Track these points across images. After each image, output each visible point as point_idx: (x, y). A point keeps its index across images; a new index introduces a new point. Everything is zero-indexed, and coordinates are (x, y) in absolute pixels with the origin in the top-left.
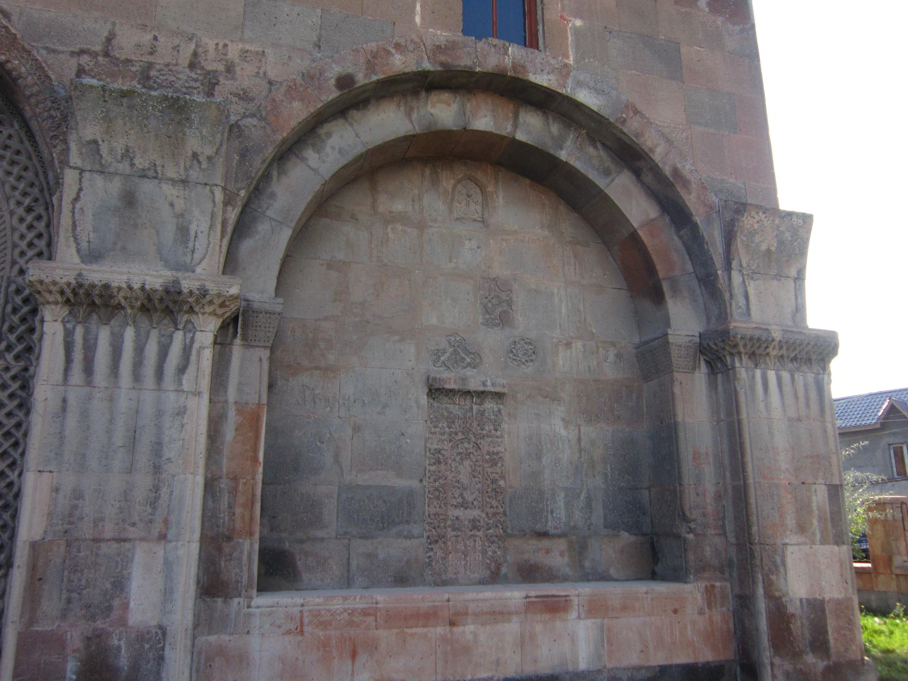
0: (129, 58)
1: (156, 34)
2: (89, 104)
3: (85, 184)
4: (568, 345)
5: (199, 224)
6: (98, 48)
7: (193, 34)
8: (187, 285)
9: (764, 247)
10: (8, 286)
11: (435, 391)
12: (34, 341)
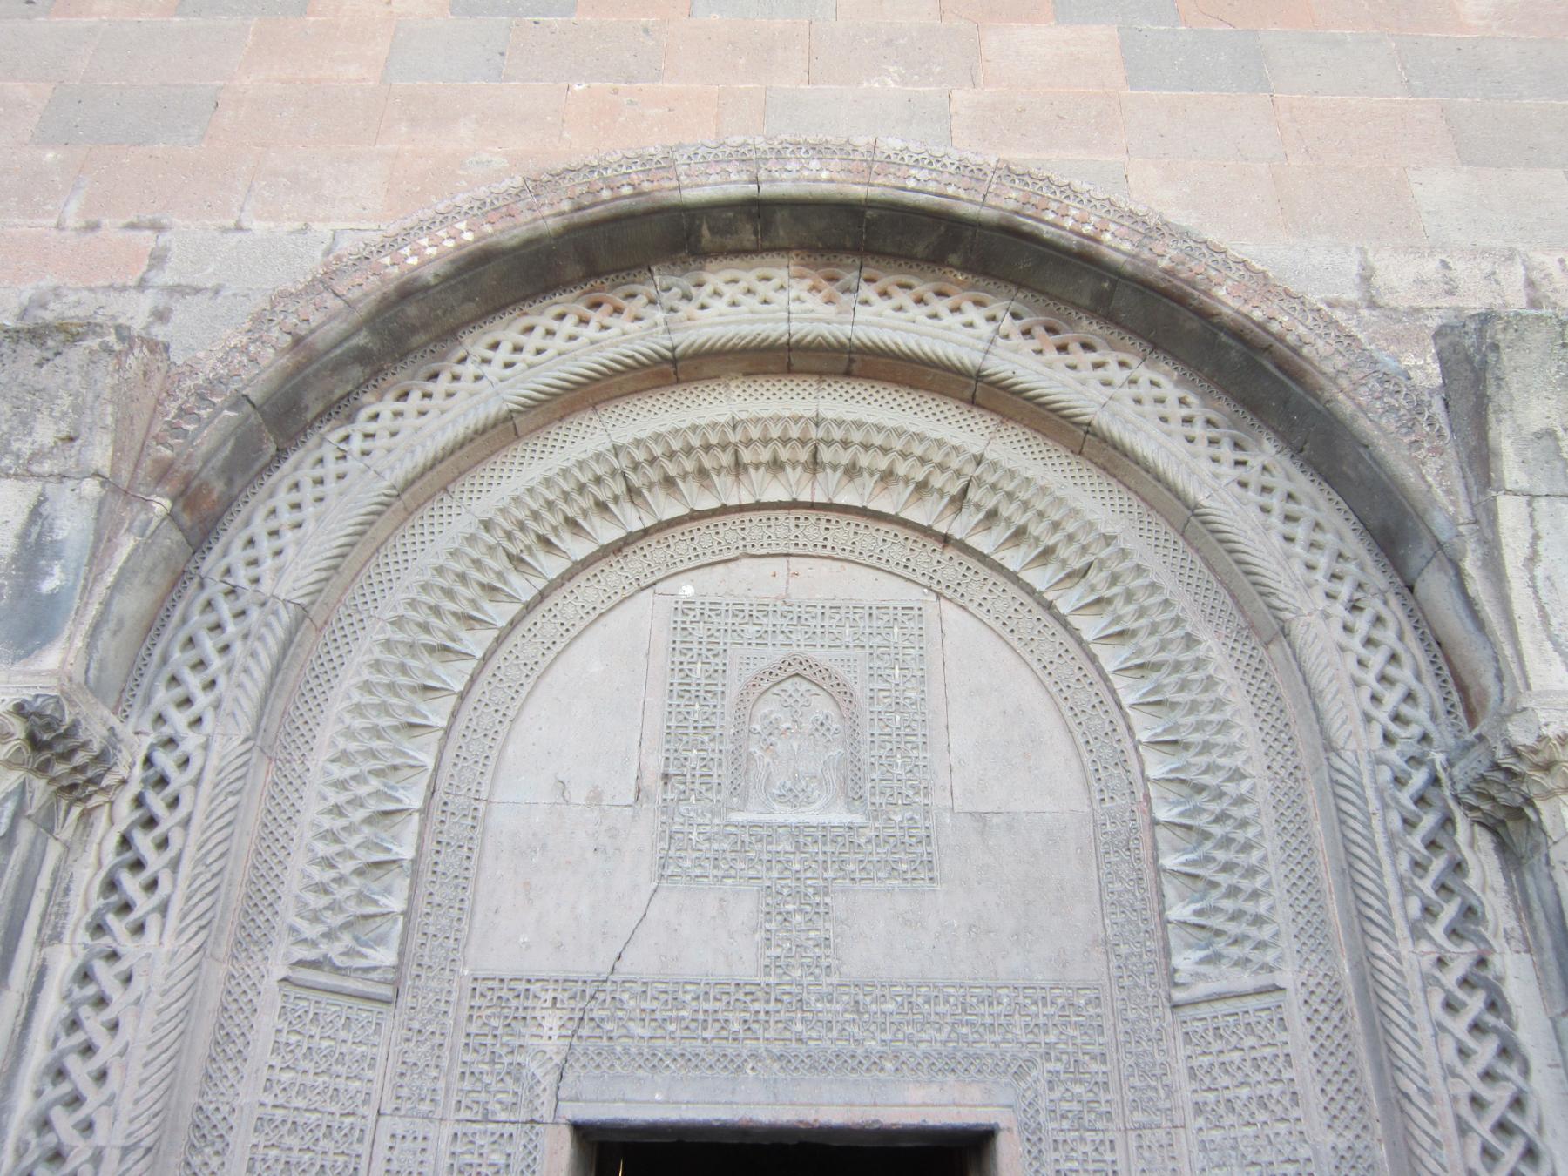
0: (1414, 304)
1: (1444, 257)
2: (1534, 356)
3: (1543, 526)
6: (1353, 295)
7: (1509, 249)
10: (1374, 774)
12: (1475, 894)
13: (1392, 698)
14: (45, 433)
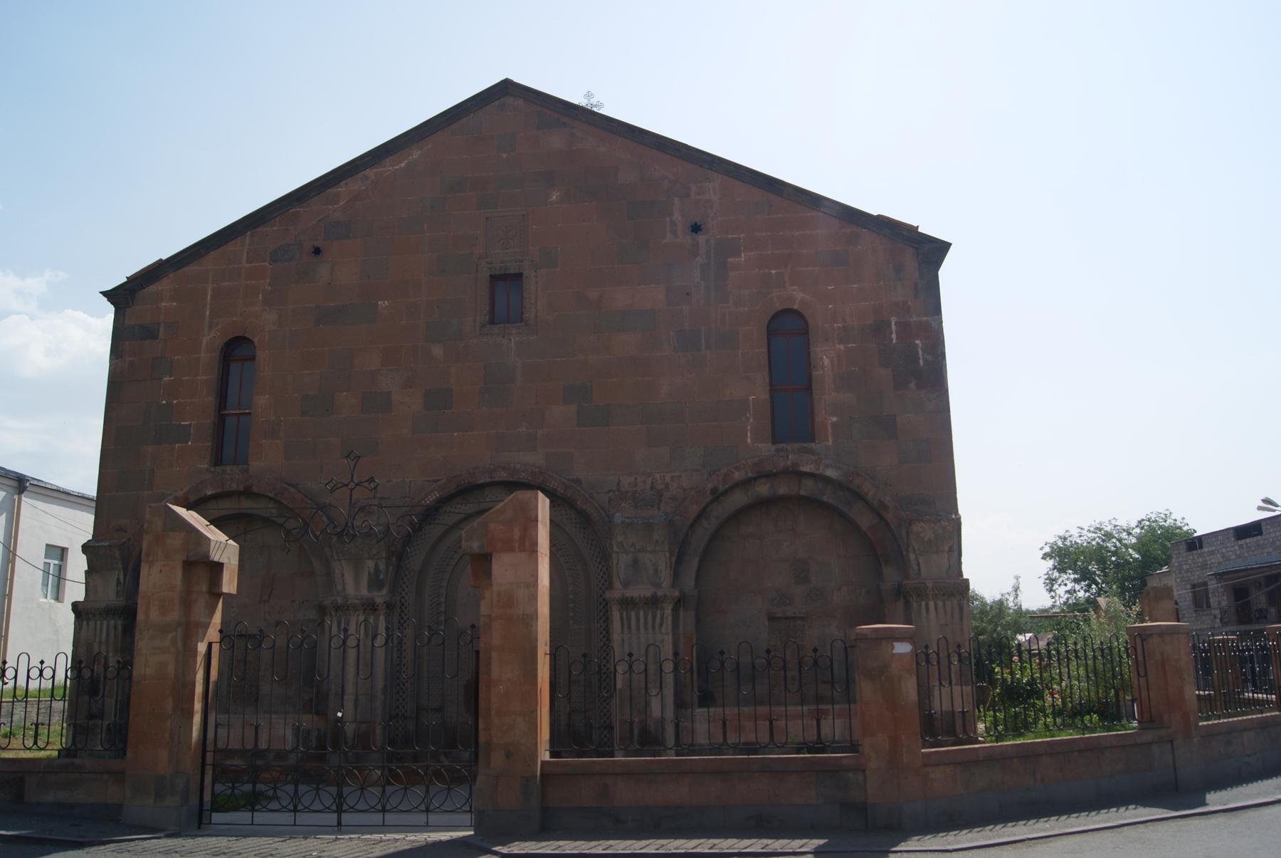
4: (839, 589)
5: (662, 566)
8: (660, 593)
9: (927, 538)
11: (772, 618)
13: (602, 581)
14: (374, 552)
